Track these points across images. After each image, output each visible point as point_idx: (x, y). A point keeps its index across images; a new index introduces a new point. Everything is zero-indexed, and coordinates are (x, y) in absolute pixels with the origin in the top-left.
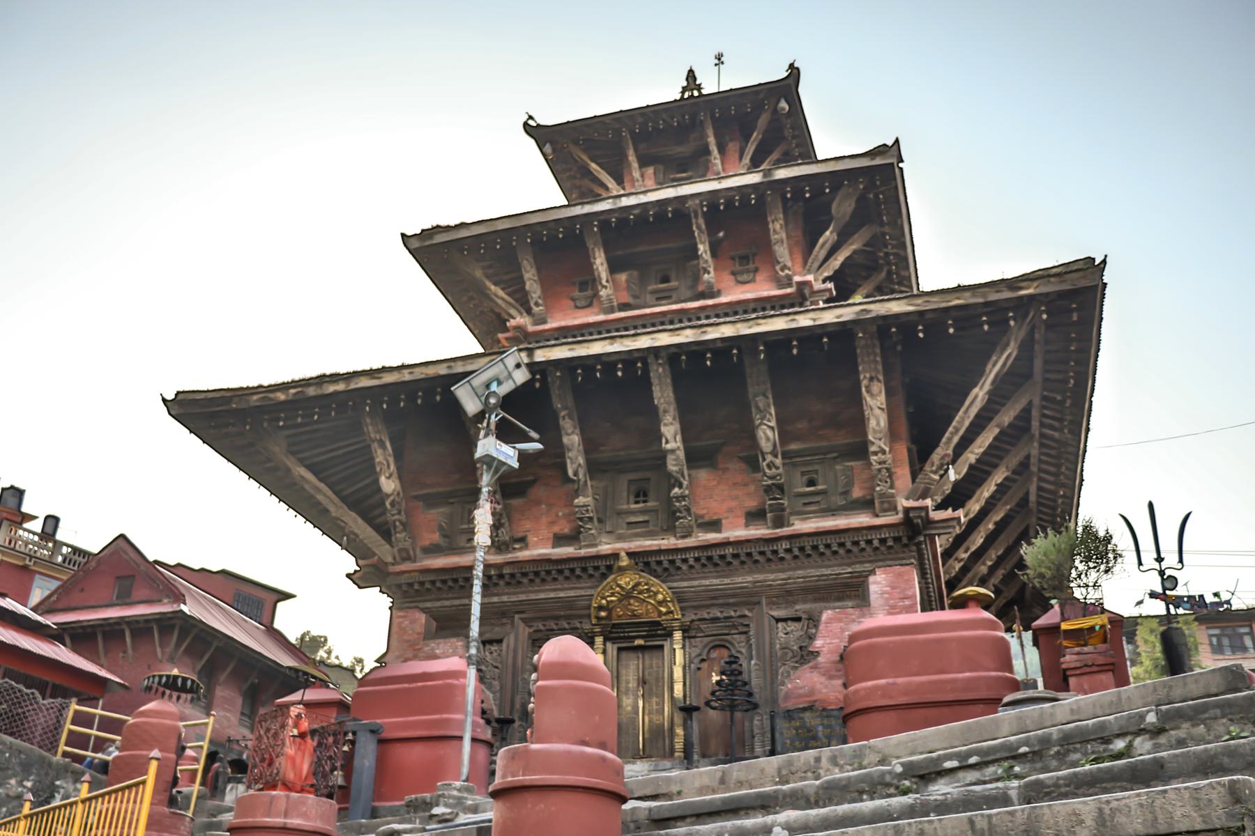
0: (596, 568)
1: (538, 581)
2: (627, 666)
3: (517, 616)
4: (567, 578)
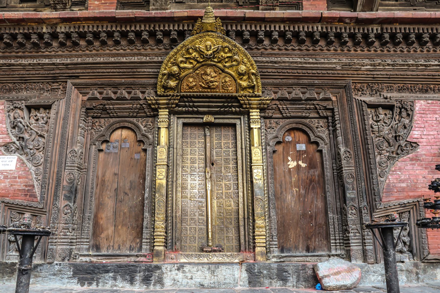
0: (167, 34)
1: (97, 44)
2: (192, 144)
3: (69, 81)
4: (131, 42)
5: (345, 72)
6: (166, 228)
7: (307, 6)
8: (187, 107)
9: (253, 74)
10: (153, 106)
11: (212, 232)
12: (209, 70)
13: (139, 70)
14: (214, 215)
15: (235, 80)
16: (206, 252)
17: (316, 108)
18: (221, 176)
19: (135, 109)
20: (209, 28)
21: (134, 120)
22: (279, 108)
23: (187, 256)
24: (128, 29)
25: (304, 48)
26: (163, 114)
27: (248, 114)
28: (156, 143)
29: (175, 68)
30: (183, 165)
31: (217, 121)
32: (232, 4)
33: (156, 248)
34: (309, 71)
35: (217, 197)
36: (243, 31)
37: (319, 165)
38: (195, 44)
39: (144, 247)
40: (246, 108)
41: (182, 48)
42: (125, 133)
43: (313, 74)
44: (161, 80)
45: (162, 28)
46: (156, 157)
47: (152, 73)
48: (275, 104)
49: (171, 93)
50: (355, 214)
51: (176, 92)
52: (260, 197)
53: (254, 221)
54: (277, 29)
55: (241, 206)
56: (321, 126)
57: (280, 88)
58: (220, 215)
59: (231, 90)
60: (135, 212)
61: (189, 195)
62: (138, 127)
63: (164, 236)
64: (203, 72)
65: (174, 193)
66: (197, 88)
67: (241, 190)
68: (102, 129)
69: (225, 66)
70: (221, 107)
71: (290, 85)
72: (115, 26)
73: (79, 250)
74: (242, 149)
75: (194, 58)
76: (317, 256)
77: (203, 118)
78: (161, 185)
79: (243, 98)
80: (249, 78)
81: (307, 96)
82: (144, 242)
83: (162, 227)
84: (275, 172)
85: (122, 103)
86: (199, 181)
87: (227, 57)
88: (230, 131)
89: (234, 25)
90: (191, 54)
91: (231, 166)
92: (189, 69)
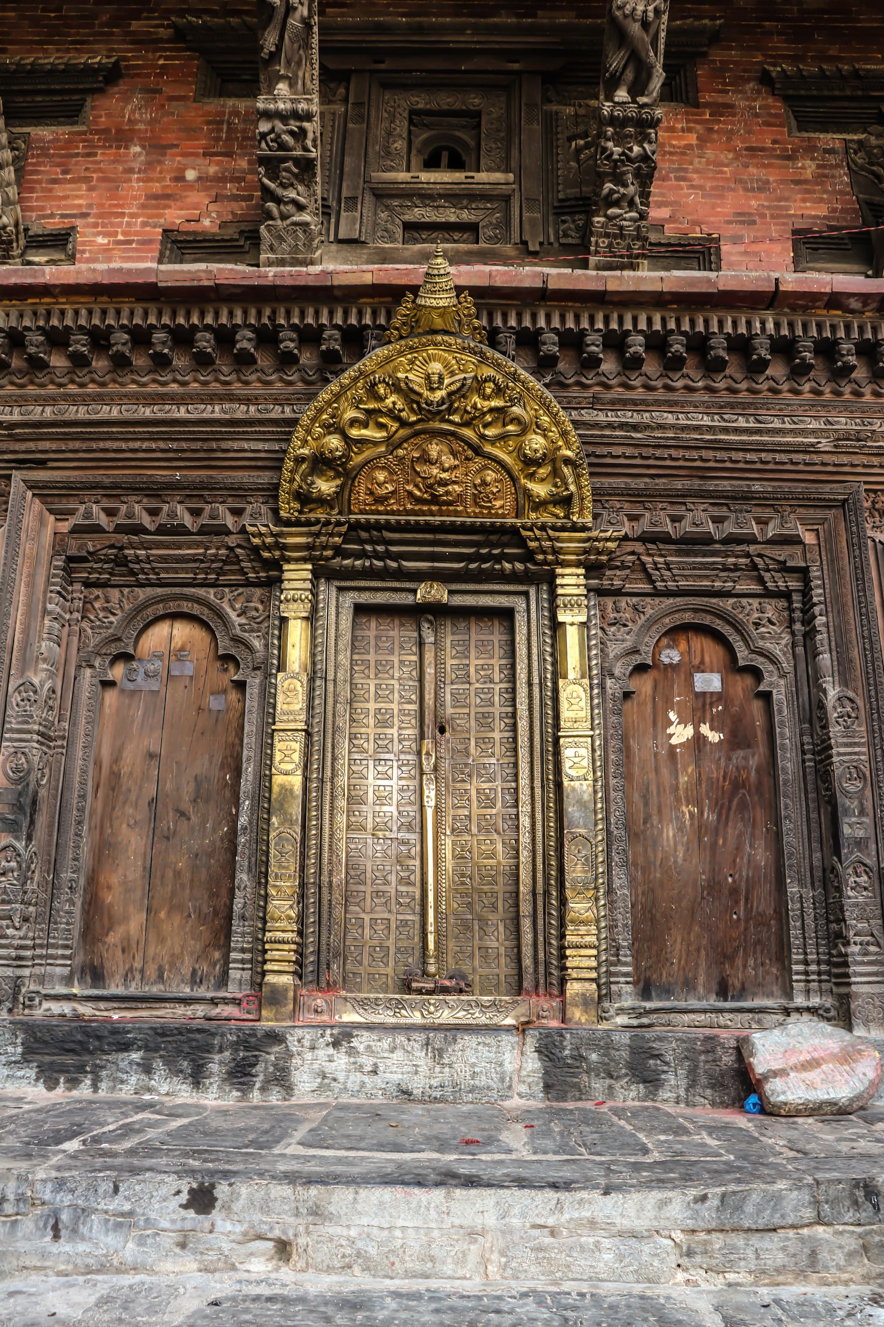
0: (310, 336)
1: (100, 364)
2: (382, 668)
3: (17, 476)
4: (203, 361)
5: (845, 459)
6: (301, 919)
7: (733, 258)
8: (369, 557)
9: (567, 461)
10: (266, 555)
11: (437, 932)
12: (434, 449)
13: (225, 445)
14: (444, 884)
15: (514, 480)
16: (419, 992)
17: (754, 567)
18: (466, 765)
19: (213, 561)
20: (439, 323)
21: (210, 594)
22: (643, 564)
23: (363, 1004)
24: (195, 320)
25: (721, 385)
26: (296, 576)
27: (551, 580)
28: (273, 665)
29: (334, 442)
30: (354, 730)
31: (458, 600)
32: (508, 249)
33: (270, 978)
34: (735, 456)
35: (453, 830)
36: (539, 332)
37: (761, 737)
38: (396, 370)
39: (235, 975)
40: (545, 562)
41: (355, 380)
42: (182, 632)
43: (747, 462)
44: (291, 478)
45: (296, 321)
46: (274, 707)
47: (263, 455)
48: (633, 553)
49: (320, 515)
50: (866, 889)
51: (336, 511)
52: (582, 831)
53: (563, 902)
54: (643, 325)
55: (525, 856)
56: (770, 621)
57: (648, 505)
58: (463, 883)
59: (502, 507)
60: (209, 869)
61: (370, 820)
62: (220, 615)
63: (294, 943)
64: (416, 455)
65: (327, 816)
66: (398, 502)
67: (525, 808)
68: (112, 619)
69: (482, 437)
70: (468, 558)
71: (677, 496)
72: (155, 311)
73: (41, 979)
74: (530, 684)
75: (390, 410)
76: (750, 1011)
77: (414, 591)
78: (286, 791)
79: (537, 532)
80: (556, 473)
81: (729, 528)
82: (236, 961)
83: (289, 918)
84: (628, 757)
85: (174, 543)
86: (400, 778)
87: (492, 410)
88: (496, 632)
89: (514, 314)
90: (381, 399)
91: (497, 735)
92: (376, 444)
